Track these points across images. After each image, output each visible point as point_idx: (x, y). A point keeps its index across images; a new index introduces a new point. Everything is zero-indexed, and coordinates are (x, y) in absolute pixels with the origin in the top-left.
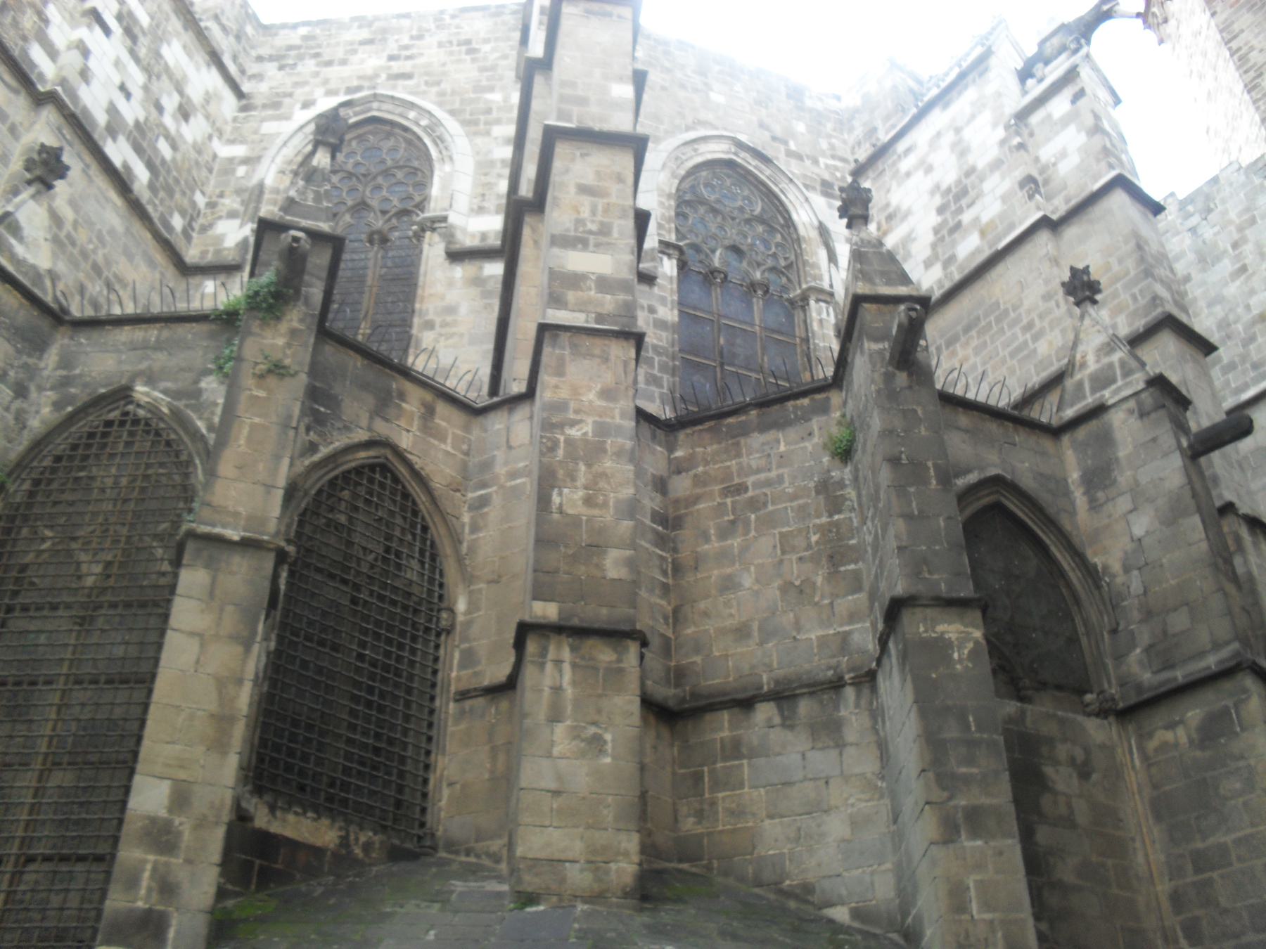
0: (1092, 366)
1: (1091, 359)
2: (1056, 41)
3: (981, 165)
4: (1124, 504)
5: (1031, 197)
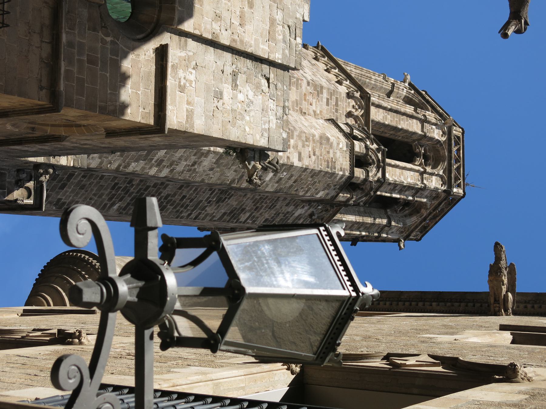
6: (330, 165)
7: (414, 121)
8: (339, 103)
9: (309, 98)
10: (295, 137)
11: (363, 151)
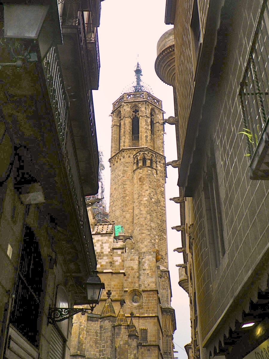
0: (121, 317)
1: (121, 316)
2: (121, 237)
3: (105, 253)
4: (120, 339)
5: (111, 266)
6: (147, 177)
9: (128, 175)
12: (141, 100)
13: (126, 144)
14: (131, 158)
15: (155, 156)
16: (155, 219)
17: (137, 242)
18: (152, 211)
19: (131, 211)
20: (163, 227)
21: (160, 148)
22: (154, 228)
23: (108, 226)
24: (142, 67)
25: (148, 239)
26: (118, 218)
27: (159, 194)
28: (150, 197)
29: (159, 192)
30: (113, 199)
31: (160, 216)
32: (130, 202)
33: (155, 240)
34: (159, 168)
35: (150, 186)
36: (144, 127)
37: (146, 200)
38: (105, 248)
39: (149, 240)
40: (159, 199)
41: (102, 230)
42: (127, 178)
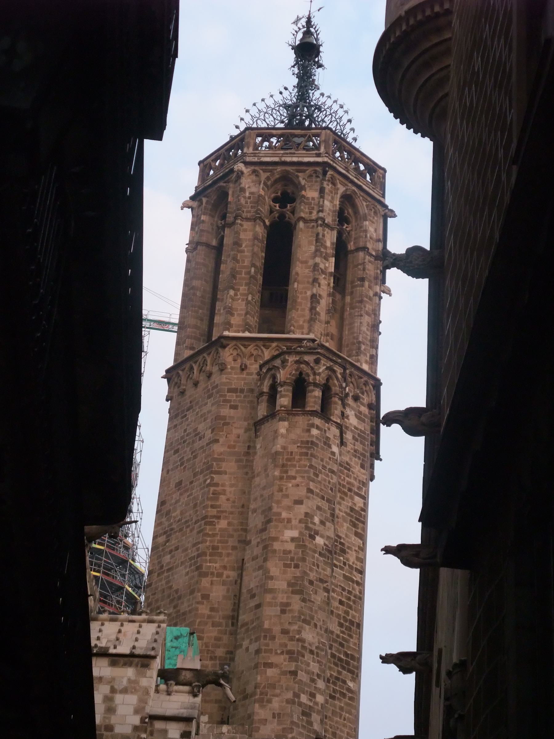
2: (188, 676)
6: (304, 450)
7: (242, 236)
8: (233, 387)
10: (279, 510)
11: (288, 391)
12: (306, 160)
13: (235, 320)
14: (251, 374)
15: (340, 376)
16: (321, 616)
17: (245, 698)
18: (311, 583)
19: (233, 574)
20: (349, 648)
21: (363, 347)
22: (314, 648)
23: (140, 626)
24: (326, 38)
25: (287, 689)
26: (180, 598)
27: (345, 520)
28: (307, 528)
29: (346, 513)
30: (167, 524)
31: (341, 602)
32: (230, 539)
33: (313, 695)
34: (353, 421)
35: (312, 486)
36: (311, 262)
37: (293, 539)
38: (121, 710)
39: (290, 695)
40: (340, 537)
41: (118, 639)
42: (229, 447)
